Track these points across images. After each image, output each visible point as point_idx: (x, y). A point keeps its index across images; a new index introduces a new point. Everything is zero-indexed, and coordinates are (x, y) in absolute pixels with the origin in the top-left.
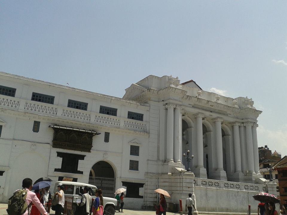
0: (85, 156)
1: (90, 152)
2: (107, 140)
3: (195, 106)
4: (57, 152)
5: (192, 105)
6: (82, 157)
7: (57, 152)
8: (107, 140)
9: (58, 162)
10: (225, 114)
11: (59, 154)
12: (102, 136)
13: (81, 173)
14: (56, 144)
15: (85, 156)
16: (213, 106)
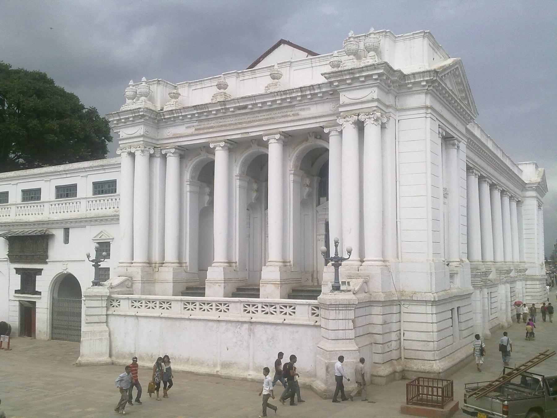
0: (42, 269)
1: (46, 263)
2: (66, 241)
3: (202, 127)
4: (15, 269)
5: (194, 126)
6: (39, 272)
7: (15, 269)
8: (66, 241)
9: (16, 281)
10: (288, 113)
11: (18, 271)
12: (59, 234)
13: (39, 293)
14: (13, 258)
15: (42, 269)
16: (245, 107)
